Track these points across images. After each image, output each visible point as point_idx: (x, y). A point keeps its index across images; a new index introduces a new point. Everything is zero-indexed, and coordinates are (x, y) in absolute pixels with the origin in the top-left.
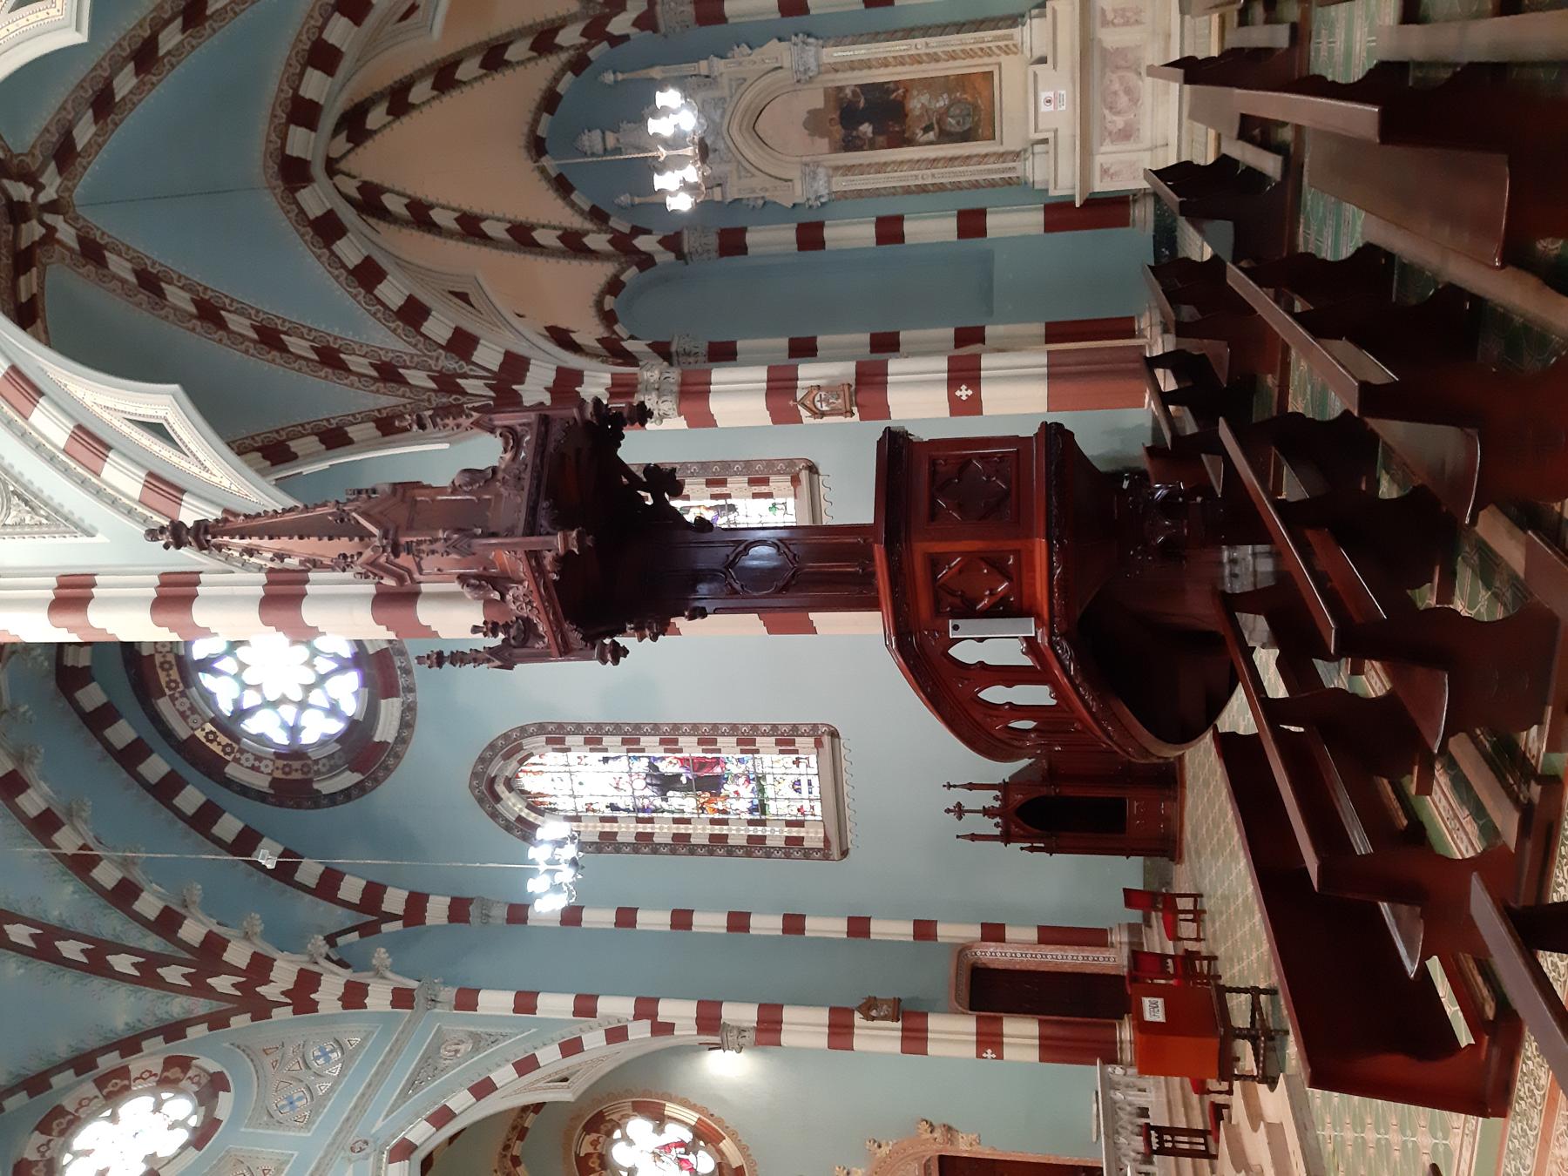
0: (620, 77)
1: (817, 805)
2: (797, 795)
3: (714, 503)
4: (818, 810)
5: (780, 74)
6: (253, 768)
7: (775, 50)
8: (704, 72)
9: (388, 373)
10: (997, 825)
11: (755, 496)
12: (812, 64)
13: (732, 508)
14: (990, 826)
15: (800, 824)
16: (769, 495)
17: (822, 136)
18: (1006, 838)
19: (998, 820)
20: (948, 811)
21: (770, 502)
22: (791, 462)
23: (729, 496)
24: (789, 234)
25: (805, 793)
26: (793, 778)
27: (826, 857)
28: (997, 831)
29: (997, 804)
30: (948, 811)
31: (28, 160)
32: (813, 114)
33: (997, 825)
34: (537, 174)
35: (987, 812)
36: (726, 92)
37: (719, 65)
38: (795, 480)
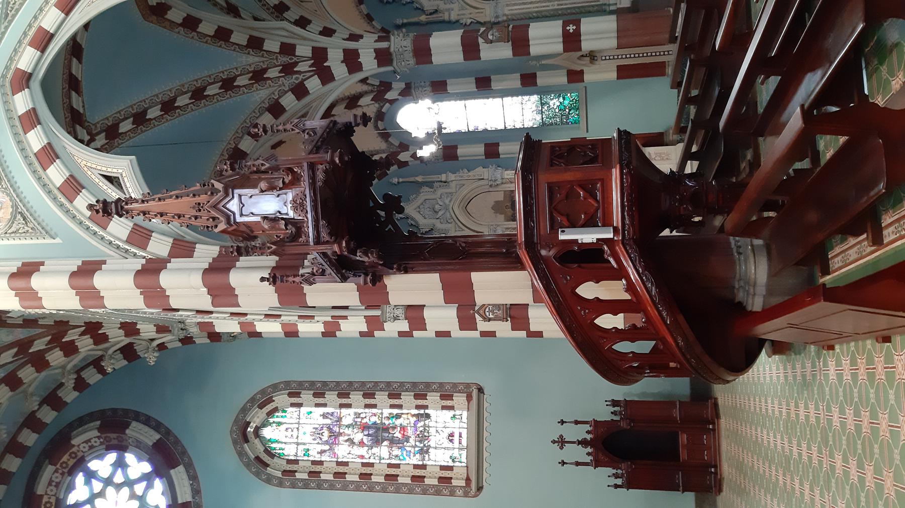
0: (401, 180)
1: (464, 453)
2: (450, 445)
3: (416, 412)
4: (464, 459)
5: (481, 182)
6: (89, 441)
7: (480, 171)
8: (443, 179)
9: (258, 76)
10: (588, 454)
11: (444, 408)
12: (499, 176)
13: (428, 416)
14: (583, 454)
15: (450, 468)
16: (451, 408)
17: (501, 213)
18: (597, 463)
19: (589, 450)
20: (554, 442)
21: (452, 413)
22: (468, 385)
23: (426, 407)
24: (480, 149)
25: (456, 444)
26: (449, 431)
27: (466, 495)
28: (588, 459)
29: (589, 437)
30: (554, 442)
31: (93, 127)
32: (497, 203)
33: (588, 454)
34: (357, 13)
35: (583, 443)
36: (454, 190)
37: (452, 177)
38: (469, 398)
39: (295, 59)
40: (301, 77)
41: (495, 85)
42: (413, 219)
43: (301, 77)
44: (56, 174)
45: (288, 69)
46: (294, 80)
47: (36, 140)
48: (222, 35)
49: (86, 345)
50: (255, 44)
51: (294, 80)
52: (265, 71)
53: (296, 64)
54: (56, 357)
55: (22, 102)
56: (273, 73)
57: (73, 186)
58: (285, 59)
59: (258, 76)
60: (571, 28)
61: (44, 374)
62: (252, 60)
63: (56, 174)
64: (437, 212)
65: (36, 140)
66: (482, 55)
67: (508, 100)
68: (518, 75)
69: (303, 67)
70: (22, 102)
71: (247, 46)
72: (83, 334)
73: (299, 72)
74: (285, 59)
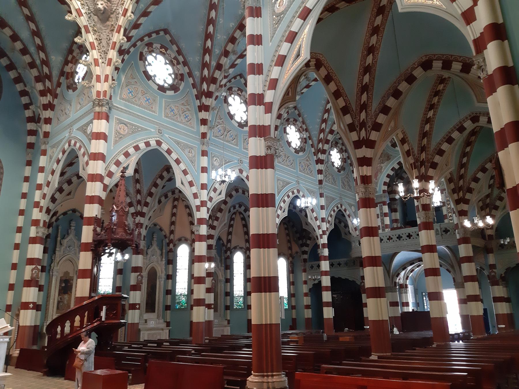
32: (69, 273)
39: (142, 205)
40: (136, 206)
41: (119, 276)
42: (67, 237)
43: (136, 206)
44: (131, 150)
45: (139, 202)
46: (135, 203)
47: (142, 145)
48: (156, 185)
49: (44, 100)
50: (150, 194)
51: (135, 203)
52: (140, 194)
53: (140, 205)
54: (40, 86)
55: (153, 143)
56: (139, 197)
57: (127, 155)
58: (143, 202)
59: (138, 192)
60: (138, 306)
61: (33, 79)
62: (145, 191)
63: (131, 150)
64: (69, 247)
65: (142, 145)
66: (133, 274)
67: (112, 280)
68: (121, 285)
69: (139, 208)
70: (153, 143)
71: (150, 191)
72: (49, 102)
73: (137, 205)
74: (143, 202)
